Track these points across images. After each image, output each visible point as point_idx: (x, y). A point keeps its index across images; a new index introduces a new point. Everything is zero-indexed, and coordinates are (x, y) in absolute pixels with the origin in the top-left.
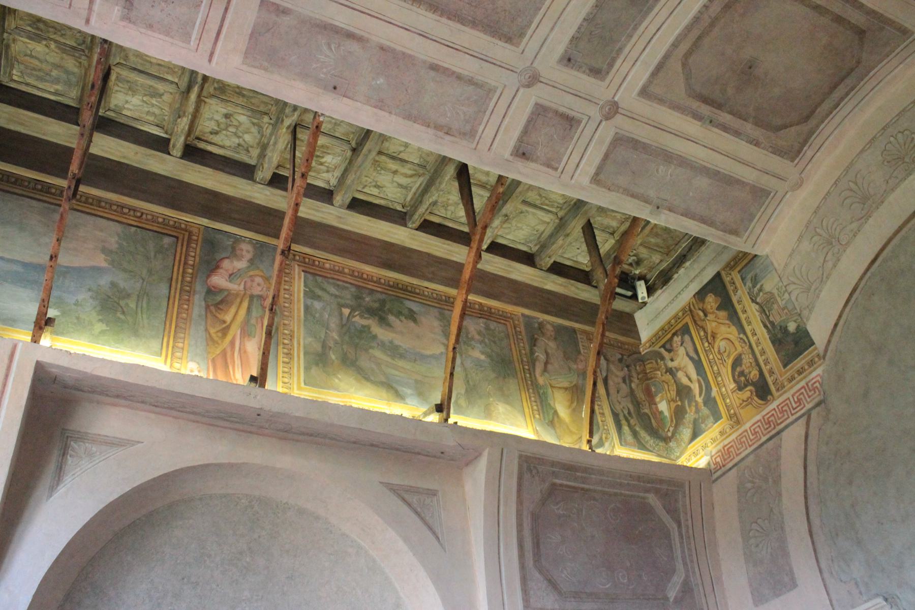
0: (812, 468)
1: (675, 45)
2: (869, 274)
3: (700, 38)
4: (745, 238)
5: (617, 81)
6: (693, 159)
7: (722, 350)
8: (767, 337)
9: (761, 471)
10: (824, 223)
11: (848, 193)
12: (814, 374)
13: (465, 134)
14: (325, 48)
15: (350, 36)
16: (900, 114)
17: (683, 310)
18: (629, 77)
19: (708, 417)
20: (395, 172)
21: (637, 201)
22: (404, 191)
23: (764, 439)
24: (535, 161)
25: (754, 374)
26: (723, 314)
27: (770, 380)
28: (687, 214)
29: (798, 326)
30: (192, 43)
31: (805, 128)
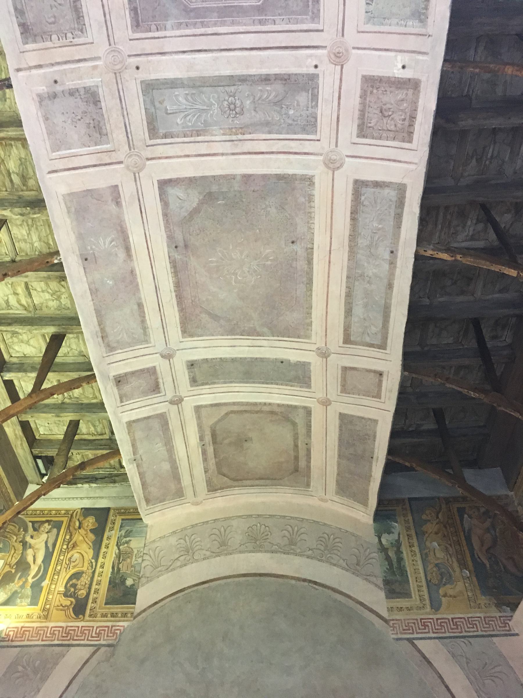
0: (75, 686)
1: (234, 404)
2: (196, 588)
3: (246, 411)
4: (149, 508)
5: (195, 393)
6: (176, 453)
7: (73, 559)
8: (110, 575)
9: (36, 665)
10: (193, 537)
11: (217, 532)
12: (121, 624)
13: (109, 346)
14: (109, 239)
15: (128, 249)
16: (271, 516)
17: (67, 511)
18: (201, 396)
19: (27, 597)
20: (16, 294)
21: (131, 449)
22: (4, 305)
23: (56, 642)
24: (119, 389)
25: (82, 593)
26: (92, 536)
27: (90, 605)
28: (142, 475)
29: (133, 585)
30: (54, 154)
31: (230, 482)
